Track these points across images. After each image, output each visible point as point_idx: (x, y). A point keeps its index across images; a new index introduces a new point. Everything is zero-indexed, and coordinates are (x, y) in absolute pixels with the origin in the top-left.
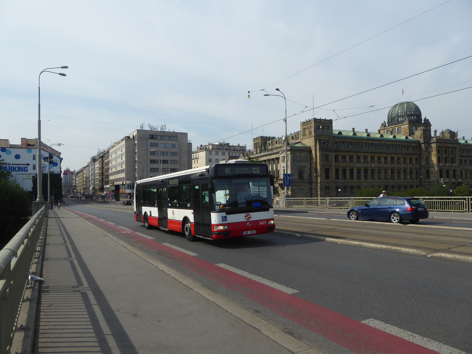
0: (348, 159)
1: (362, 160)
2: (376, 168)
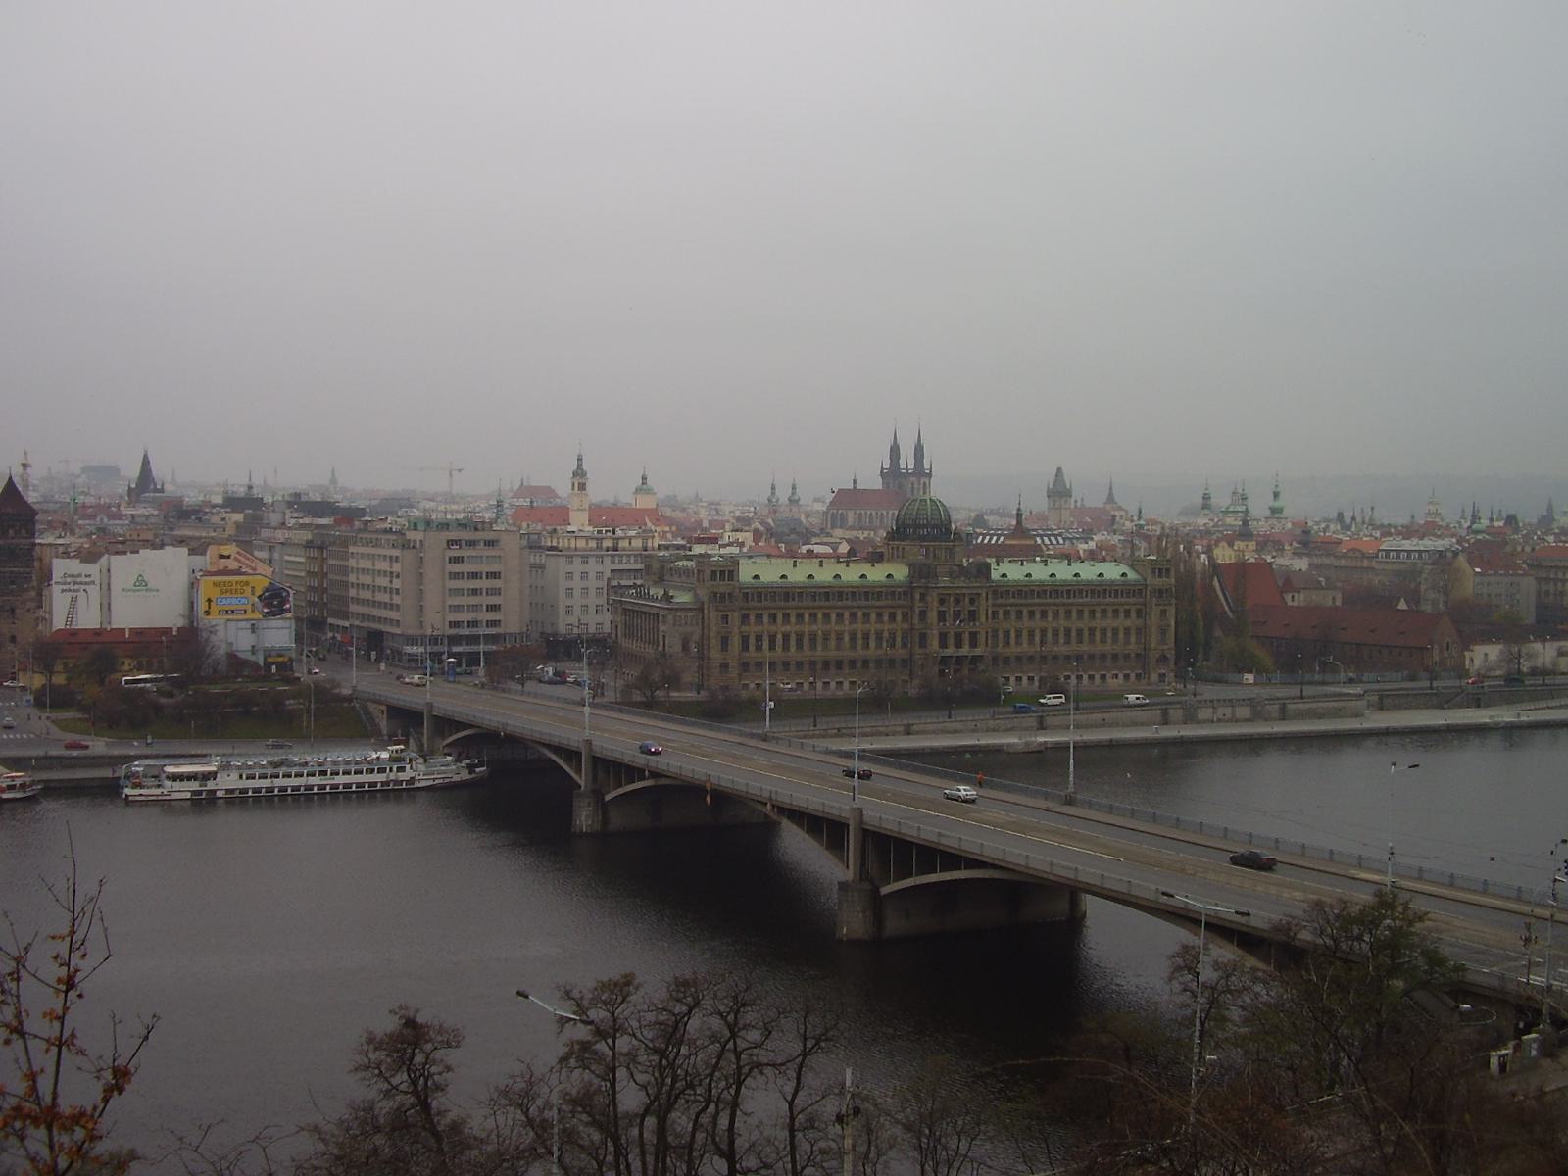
0: (766, 619)
1: (793, 620)
2: (820, 632)
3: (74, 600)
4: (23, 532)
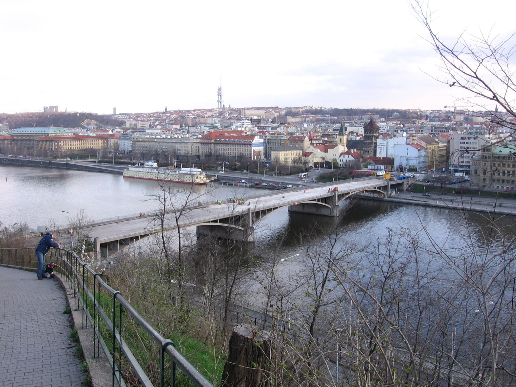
1: (511, 166)
3: (381, 150)
4: (371, 133)
